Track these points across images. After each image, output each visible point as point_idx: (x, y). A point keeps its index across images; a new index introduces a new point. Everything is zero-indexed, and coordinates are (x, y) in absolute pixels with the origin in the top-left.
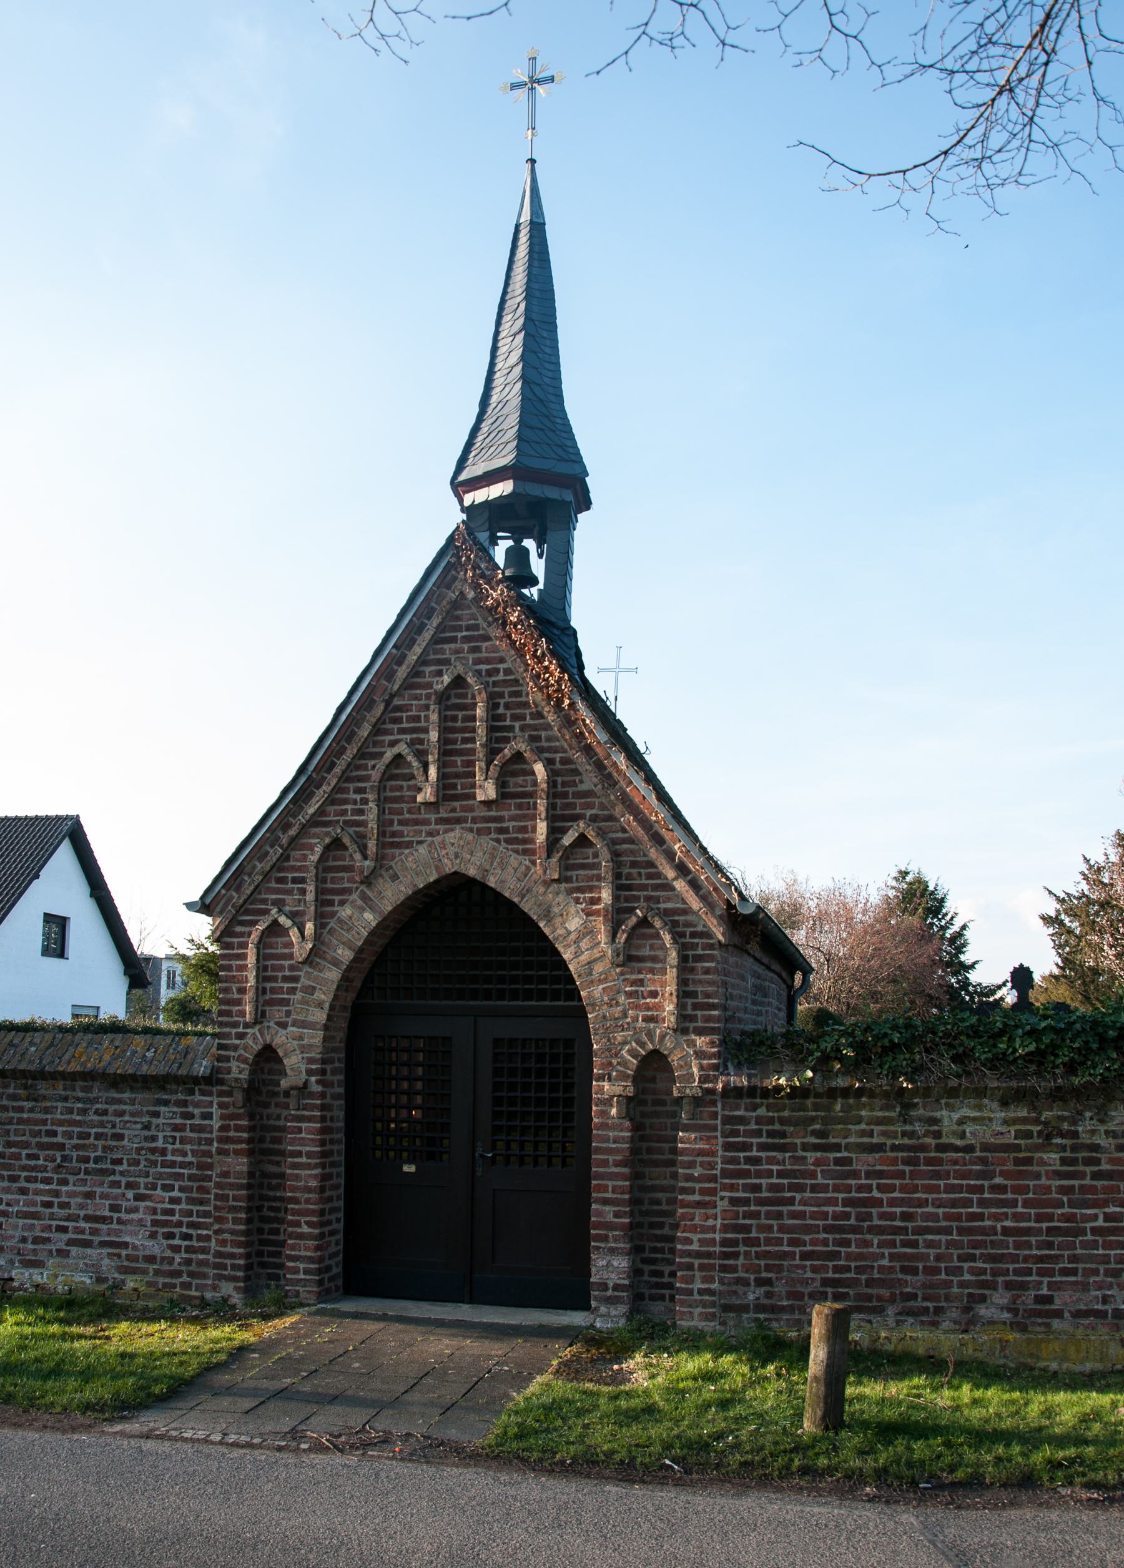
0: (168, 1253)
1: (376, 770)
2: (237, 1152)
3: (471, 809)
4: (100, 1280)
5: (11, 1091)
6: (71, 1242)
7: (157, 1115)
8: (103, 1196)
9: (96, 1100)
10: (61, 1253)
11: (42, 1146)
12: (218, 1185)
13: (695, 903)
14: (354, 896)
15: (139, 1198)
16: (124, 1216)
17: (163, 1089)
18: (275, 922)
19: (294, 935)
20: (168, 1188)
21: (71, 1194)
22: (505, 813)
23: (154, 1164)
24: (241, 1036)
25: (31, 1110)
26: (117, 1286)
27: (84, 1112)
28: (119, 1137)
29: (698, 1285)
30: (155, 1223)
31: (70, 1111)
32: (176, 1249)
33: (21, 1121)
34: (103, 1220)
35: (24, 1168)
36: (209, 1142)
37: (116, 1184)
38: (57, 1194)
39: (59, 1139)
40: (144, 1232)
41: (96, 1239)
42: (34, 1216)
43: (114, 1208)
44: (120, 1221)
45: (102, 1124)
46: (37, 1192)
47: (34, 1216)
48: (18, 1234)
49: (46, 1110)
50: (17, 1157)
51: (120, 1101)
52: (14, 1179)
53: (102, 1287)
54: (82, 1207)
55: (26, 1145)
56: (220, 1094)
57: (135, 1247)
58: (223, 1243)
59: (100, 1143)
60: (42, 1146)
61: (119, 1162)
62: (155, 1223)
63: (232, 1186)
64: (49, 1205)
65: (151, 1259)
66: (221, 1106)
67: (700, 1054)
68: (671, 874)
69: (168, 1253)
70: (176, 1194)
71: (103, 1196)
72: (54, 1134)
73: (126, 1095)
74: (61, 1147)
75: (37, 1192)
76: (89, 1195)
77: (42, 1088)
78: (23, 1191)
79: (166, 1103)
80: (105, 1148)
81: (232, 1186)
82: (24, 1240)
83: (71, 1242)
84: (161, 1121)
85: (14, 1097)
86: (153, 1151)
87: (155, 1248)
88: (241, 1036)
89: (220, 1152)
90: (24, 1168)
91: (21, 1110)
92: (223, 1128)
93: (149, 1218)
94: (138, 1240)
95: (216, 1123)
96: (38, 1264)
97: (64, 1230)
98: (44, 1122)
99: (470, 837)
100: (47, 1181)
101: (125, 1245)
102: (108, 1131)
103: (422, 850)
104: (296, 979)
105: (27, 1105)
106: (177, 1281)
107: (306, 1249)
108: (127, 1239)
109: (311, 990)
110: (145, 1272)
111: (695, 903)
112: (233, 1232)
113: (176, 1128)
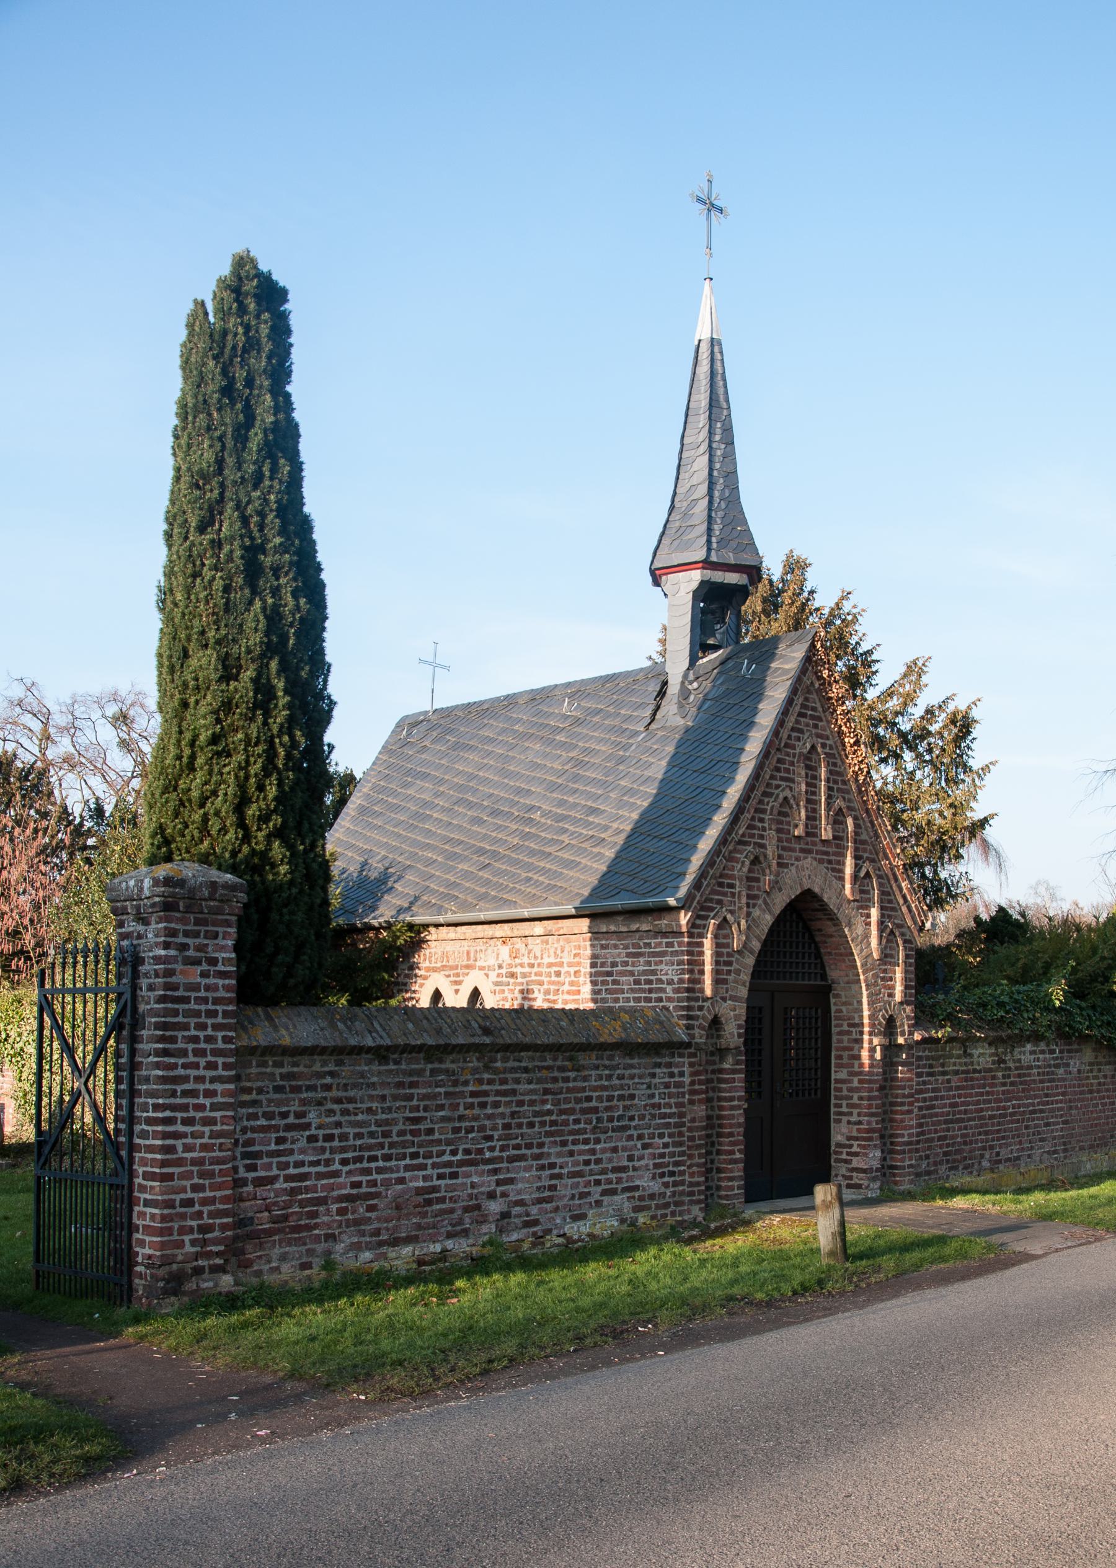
0: (663, 1190)
1: (771, 804)
2: (700, 1101)
3: (814, 844)
4: (622, 1221)
5: (559, 1063)
6: (604, 1193)
7: (653, 1075)
8: (624, 1149)
9: (616, 1067)
10: (598, 1203)
11: (584, 1111)
12: (690, 1129)
13: (909, 922)
14: (760, 902)
15: (645, 1146)
16: (637, 1164)
17: (658, 1054)
18: (725, 919)
19: (734, 928)
20: (661, 1136)
21: (604, 1151)
22: (829, 850)
23: (653, 1116)
24: (701, 1008)
25: (575, 1080)
26: (633, 1223)
27: (609, 1077)
28: (632, 1097)
29: (907, 1163)
30: (656, 1166)
31: (600, 1077)
32: (666, 1185)
33: (569, 1090)
34: (624, 1169)
35: (571, 1133)
36: (683, 1094)
37: (630, 1138)
38: (593, 1152)
39: (594, 1104)
40: (648, 1175)
41: (620, 1187)
42: (579, 1174)
43: (630, 1158)
44: (635, 1169)
45: (622, 1087)
46: (581, 1153)
47: (579, 1174)
48: (568, 1192)
49: (585, 1079)
50: (566, 1123)
51: (632, 1066)
52: (564, 1143)
53: (625, 1227)
54: (610, 1160)
55: (572, 1111)
56: (691, 1055)
57: (644, 1189)
58: (692, 1175)
59: (621, 1104)
60: (584, 1111)
61: (632, 1118)
62: (656, 1166)
63: (698, 1129)
64: (587, 1163)
65: (652, 1196)
66: (691, 1065)
67: (908, 1017)
68: (901, 901)
69: (663, 1190)
70: (666, 1140)
71: (624, 1149)
72: (589, 1099)
73: (635, 1061)
74: (595, 1110)
75: (581, 1153)
76: (615, 1150)
77: (583, 1059)
78: (571, 1154)
79: (659, 1065)
80: (626, 1108)
81: (698, 1129)
82: (573, 1197)
83: (604, 1193)
84: (657, 1080)
85: (562, 1069)
86: (653, 1106)
87: (655, 1186)
88: (701, 1008)
89: (692, 1102)
90: (571, 1133)
91: (566, 1080)
92: (692, 1083)
93: (651, 1163)
94: (648, 1183)
95: (687, 1080)
96: (582, 1217)
97: (598, 1183)
98: (583, 1089)
99: (815, 863)
100: (586, 1142)
101: (637, 1188)
102: (626, 1093)
103: (793, 869)
104: (730, 963)
105: (572, 1075)
106: (668, 1211)
107: (738, 1171)
108: (638, 1183)
109: (738, 972)
110: (648, 1208)
111: (909, 922)
112: (698, 1165)
113: (667, 1086)
